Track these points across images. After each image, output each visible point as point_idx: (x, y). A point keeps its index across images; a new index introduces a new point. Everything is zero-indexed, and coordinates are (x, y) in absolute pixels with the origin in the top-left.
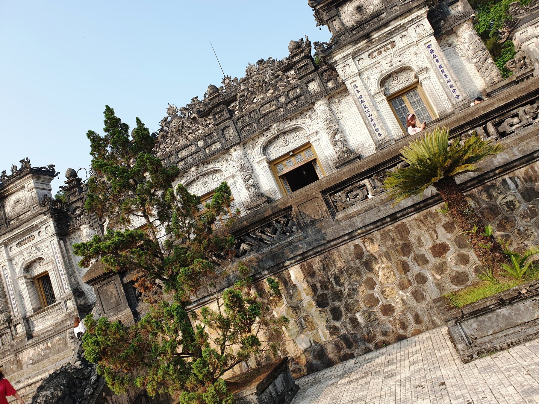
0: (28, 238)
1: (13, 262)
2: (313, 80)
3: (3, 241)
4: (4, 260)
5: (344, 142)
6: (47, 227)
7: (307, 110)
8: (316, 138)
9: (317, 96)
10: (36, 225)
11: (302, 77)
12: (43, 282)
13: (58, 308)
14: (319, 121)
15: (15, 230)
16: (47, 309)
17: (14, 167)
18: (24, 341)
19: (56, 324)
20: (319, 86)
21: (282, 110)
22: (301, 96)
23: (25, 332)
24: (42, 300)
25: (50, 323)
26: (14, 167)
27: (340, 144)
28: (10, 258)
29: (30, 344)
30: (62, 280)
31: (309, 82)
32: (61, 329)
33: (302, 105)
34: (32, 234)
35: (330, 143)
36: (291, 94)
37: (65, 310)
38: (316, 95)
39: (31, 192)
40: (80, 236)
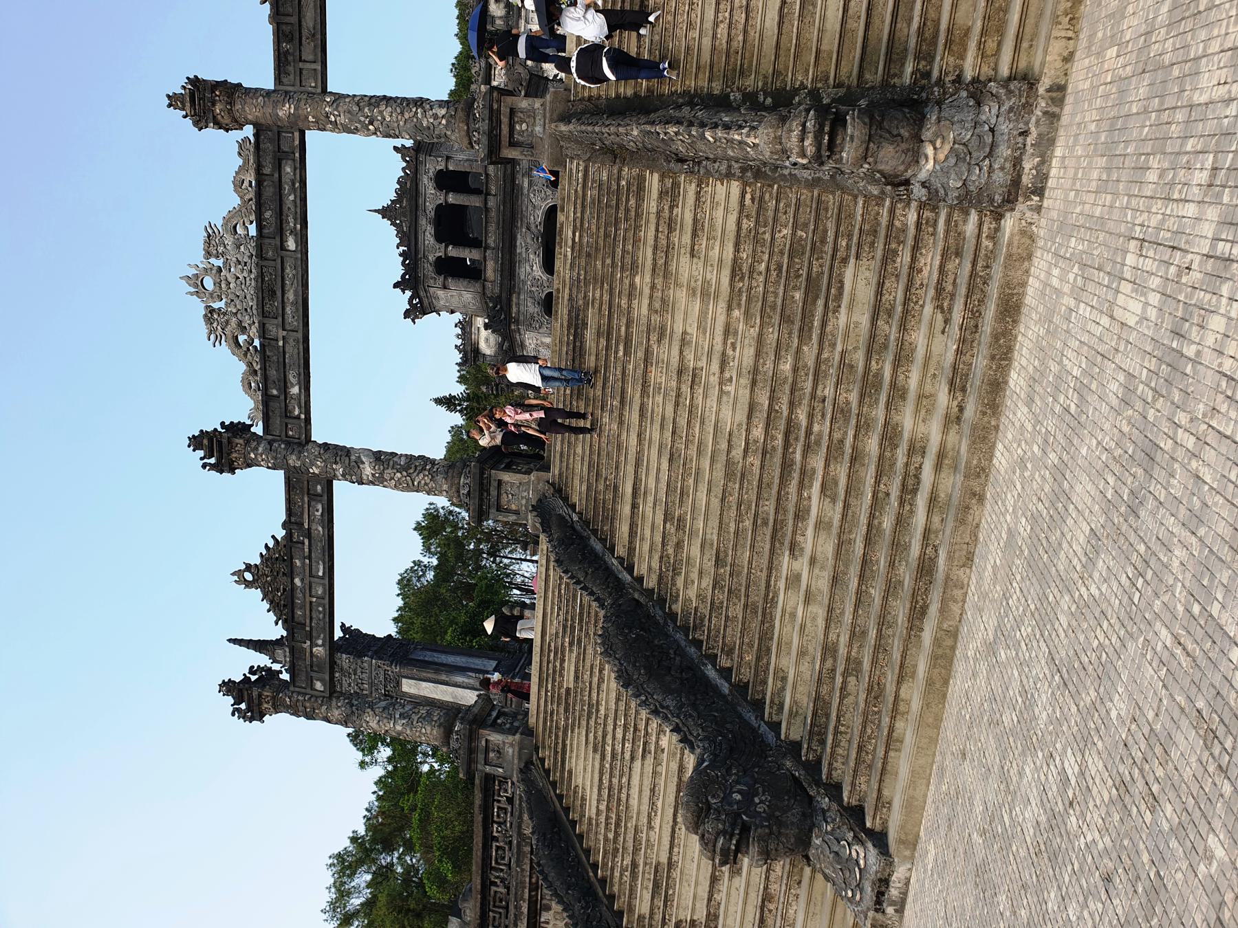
17: (458, 336)
26: (458, 336)
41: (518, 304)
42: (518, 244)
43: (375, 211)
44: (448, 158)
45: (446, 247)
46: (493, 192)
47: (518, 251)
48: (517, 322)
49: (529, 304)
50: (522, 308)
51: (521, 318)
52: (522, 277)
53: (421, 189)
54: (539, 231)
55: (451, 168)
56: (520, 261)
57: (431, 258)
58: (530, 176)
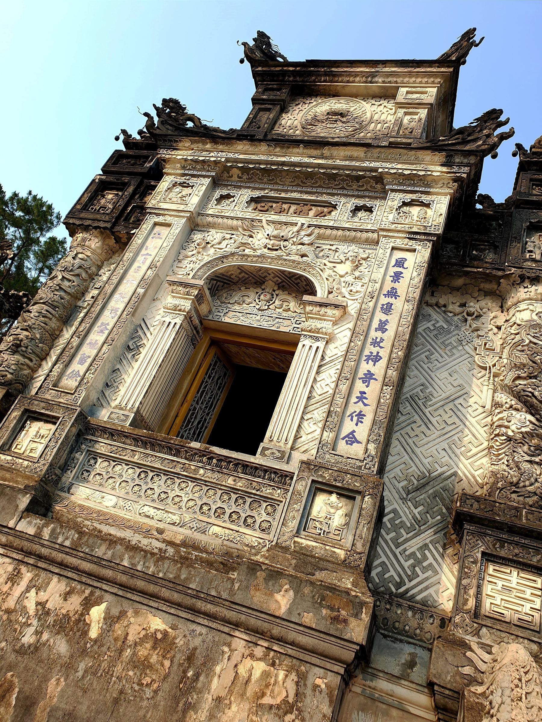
0: (306, 202)
1: (198, 237)
3: (228, 160)
4: (182, 207)
6: (410, 204)
10: (380, 179)
12: (215, 365)
13: (240, 485)
15: (301, 149)
16: (192, 455)
18: (12, 500)
19: (184, 544)
23: (42, 468)
24: (173, 414)
25: (160, 514)
28: (199, 220)
29: (21, 535)
30: (356, 393)
32: (215, 600)
34: (333, 200)
37: (293, 524)
39: (406, 114)
40: (479, 316)
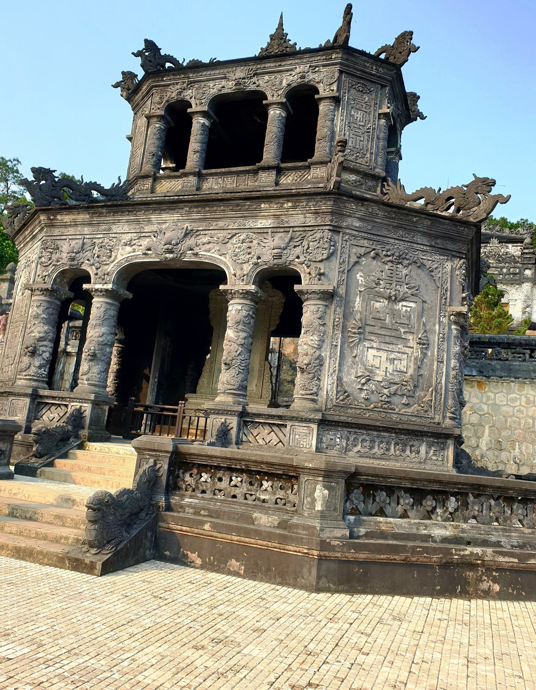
2: (530, 269)
5: (530, 314)
7: (517, 284)
8: (514, 303)
9: (527, 280)
11: (524, 264)
14: (521, 294)
20: (532, 274)
21: (501, 276)
22: (517, 274)
27: (527, 314)
31: (526, 269)
33: (516, 280)
35: (521, 311)
36: (512, 269)
38: (528, 279)
41: (75, 224)
42: (165, 216)
43: (281, 24)
44: (336, 100)
45: (204, 114)
46: (283, 180)
47: (154, 217)
48: (51, 225)
49: (73, 243)
50: (71, 230)
51: (57, 231)
52: (115, 228)
53: (287, 64)
54: (183, 254)
55: (323, 107)
56: (138, 222)
57: (188, 95)
58: (275, 230)
